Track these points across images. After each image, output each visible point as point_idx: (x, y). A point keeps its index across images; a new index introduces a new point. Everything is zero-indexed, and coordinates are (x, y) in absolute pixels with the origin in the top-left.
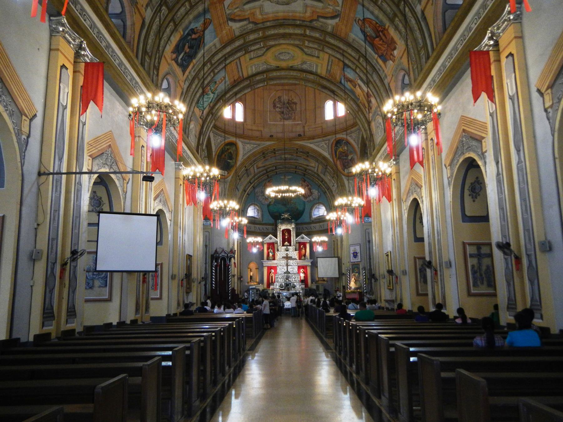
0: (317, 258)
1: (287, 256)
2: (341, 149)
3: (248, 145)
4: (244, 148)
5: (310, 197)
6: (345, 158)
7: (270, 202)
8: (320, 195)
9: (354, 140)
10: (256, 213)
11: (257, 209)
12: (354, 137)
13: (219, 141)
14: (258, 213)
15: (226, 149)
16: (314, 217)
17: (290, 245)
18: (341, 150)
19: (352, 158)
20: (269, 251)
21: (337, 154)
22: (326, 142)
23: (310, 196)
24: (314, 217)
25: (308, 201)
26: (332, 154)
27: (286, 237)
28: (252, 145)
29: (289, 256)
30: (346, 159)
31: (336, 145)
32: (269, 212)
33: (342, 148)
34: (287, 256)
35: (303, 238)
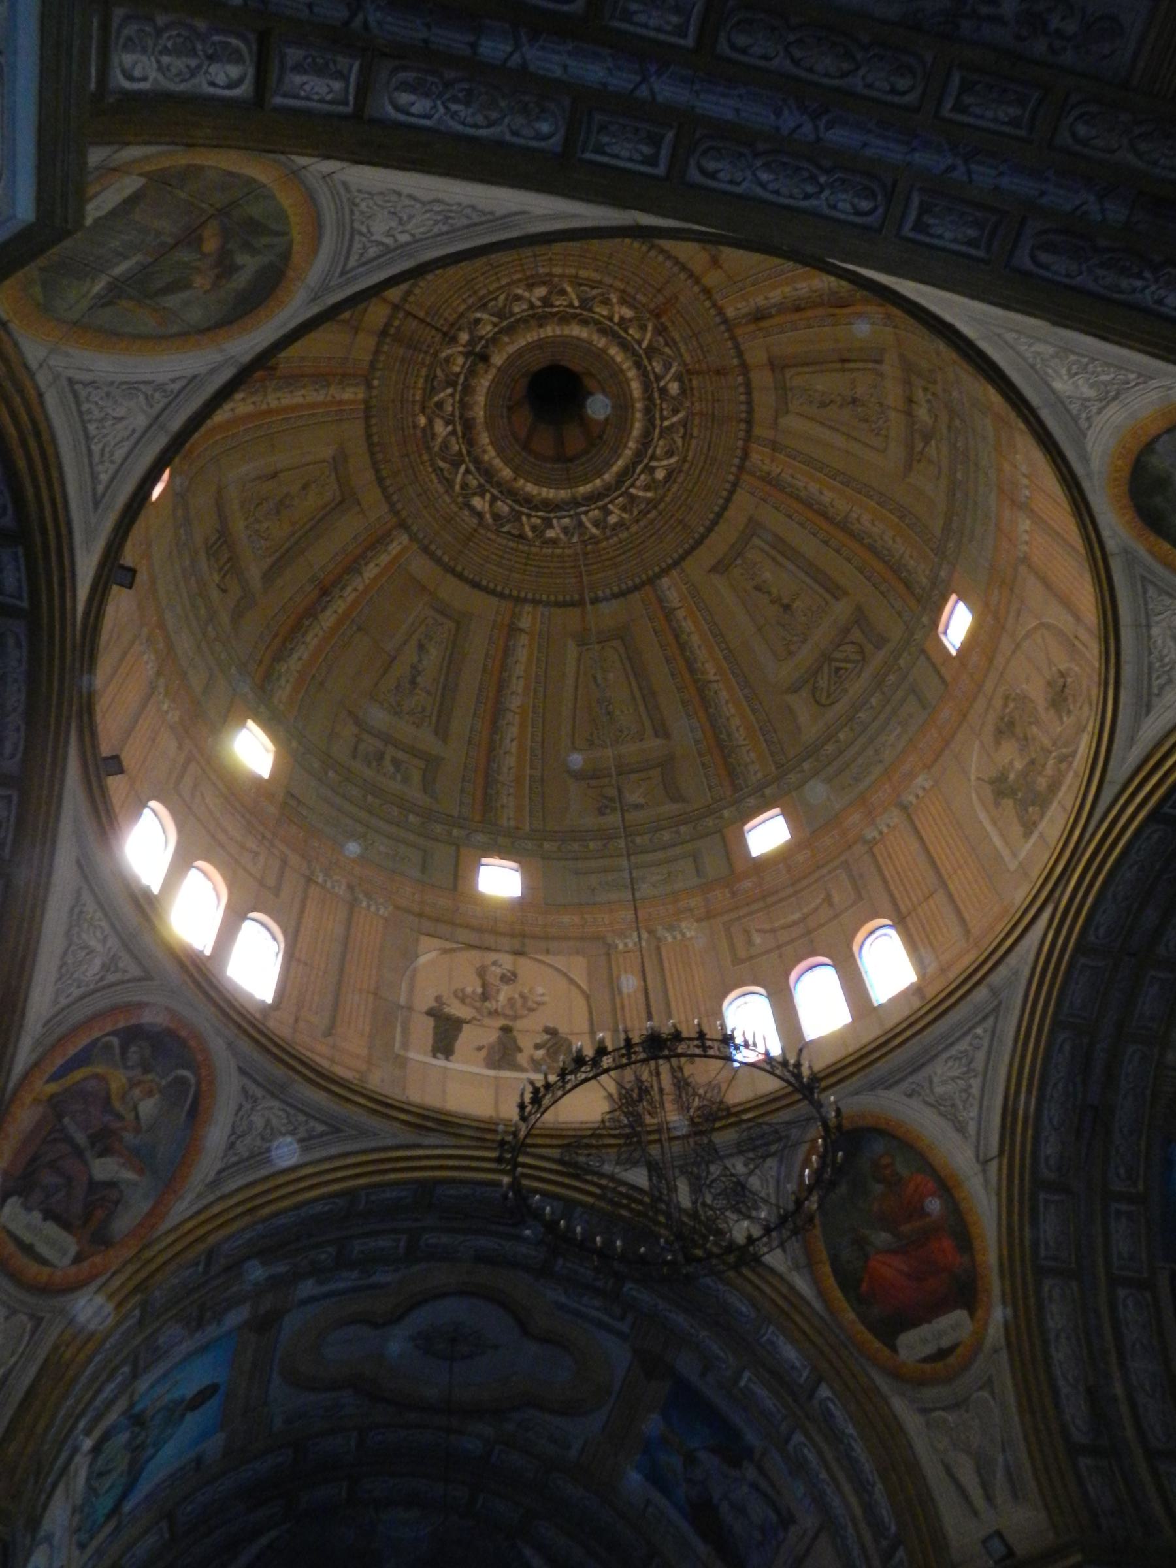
2: (118, 1080)
3: (141, 421)
4: (131, 388)
6: (81, 1138)
9: (236, 1136)
12: (258, 1120)
13: (380, 228)
15: (241, 259)
18: (114, 1086)
19: (112, 1184)
21: (78, 1075)
22: (126, 961)
26: (62, 1041)
28: (119, 454)
30: (79, 1152)
31: (132, 1034)
33: (133, 1084)
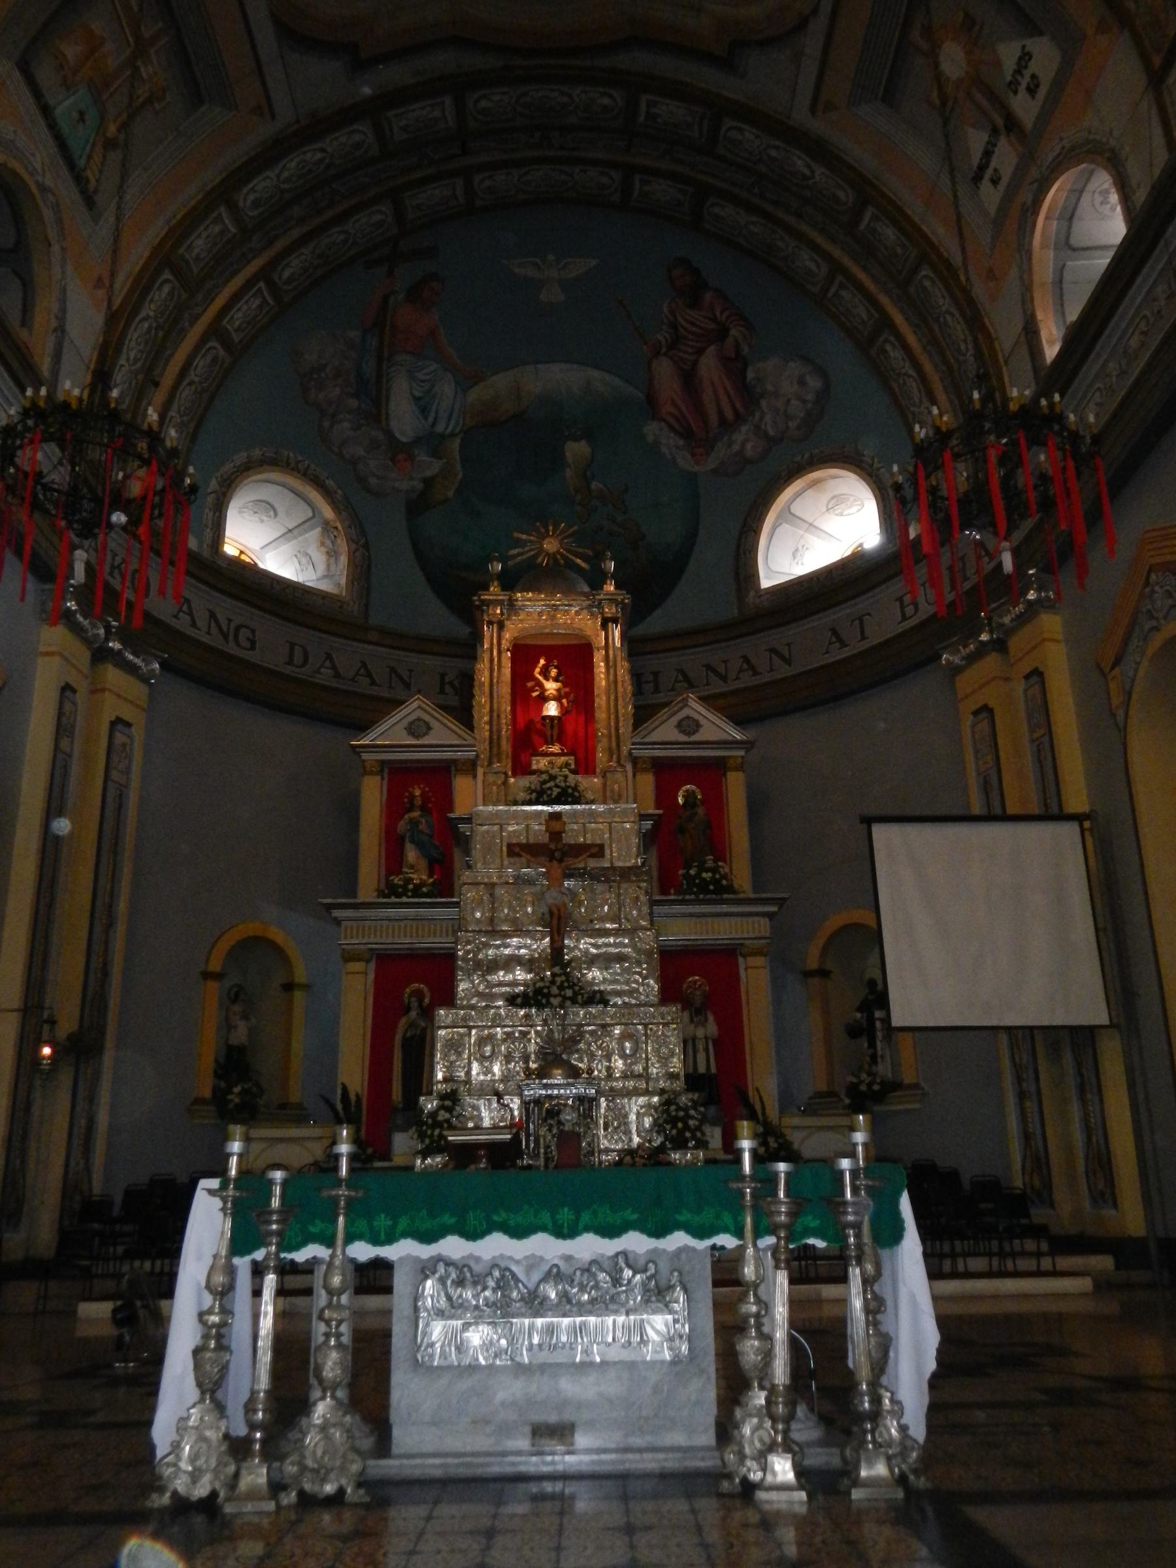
0: (868, 821)
1: (556, 836)
5: (743, 434)
7: (428, 482)
8: (824, 395)
10: (319, 557)
11: (327, 527)
14: (332, 554)
16: (766, 583)
17: (585, 766)
20: (402, 826)
23: (739, 418)
24: (766, 583)
25: (714, 472)
27: (552, 709)
29: (568, 839)
32: (420, 556)
34: (556, 836)
35: (689, 726)
